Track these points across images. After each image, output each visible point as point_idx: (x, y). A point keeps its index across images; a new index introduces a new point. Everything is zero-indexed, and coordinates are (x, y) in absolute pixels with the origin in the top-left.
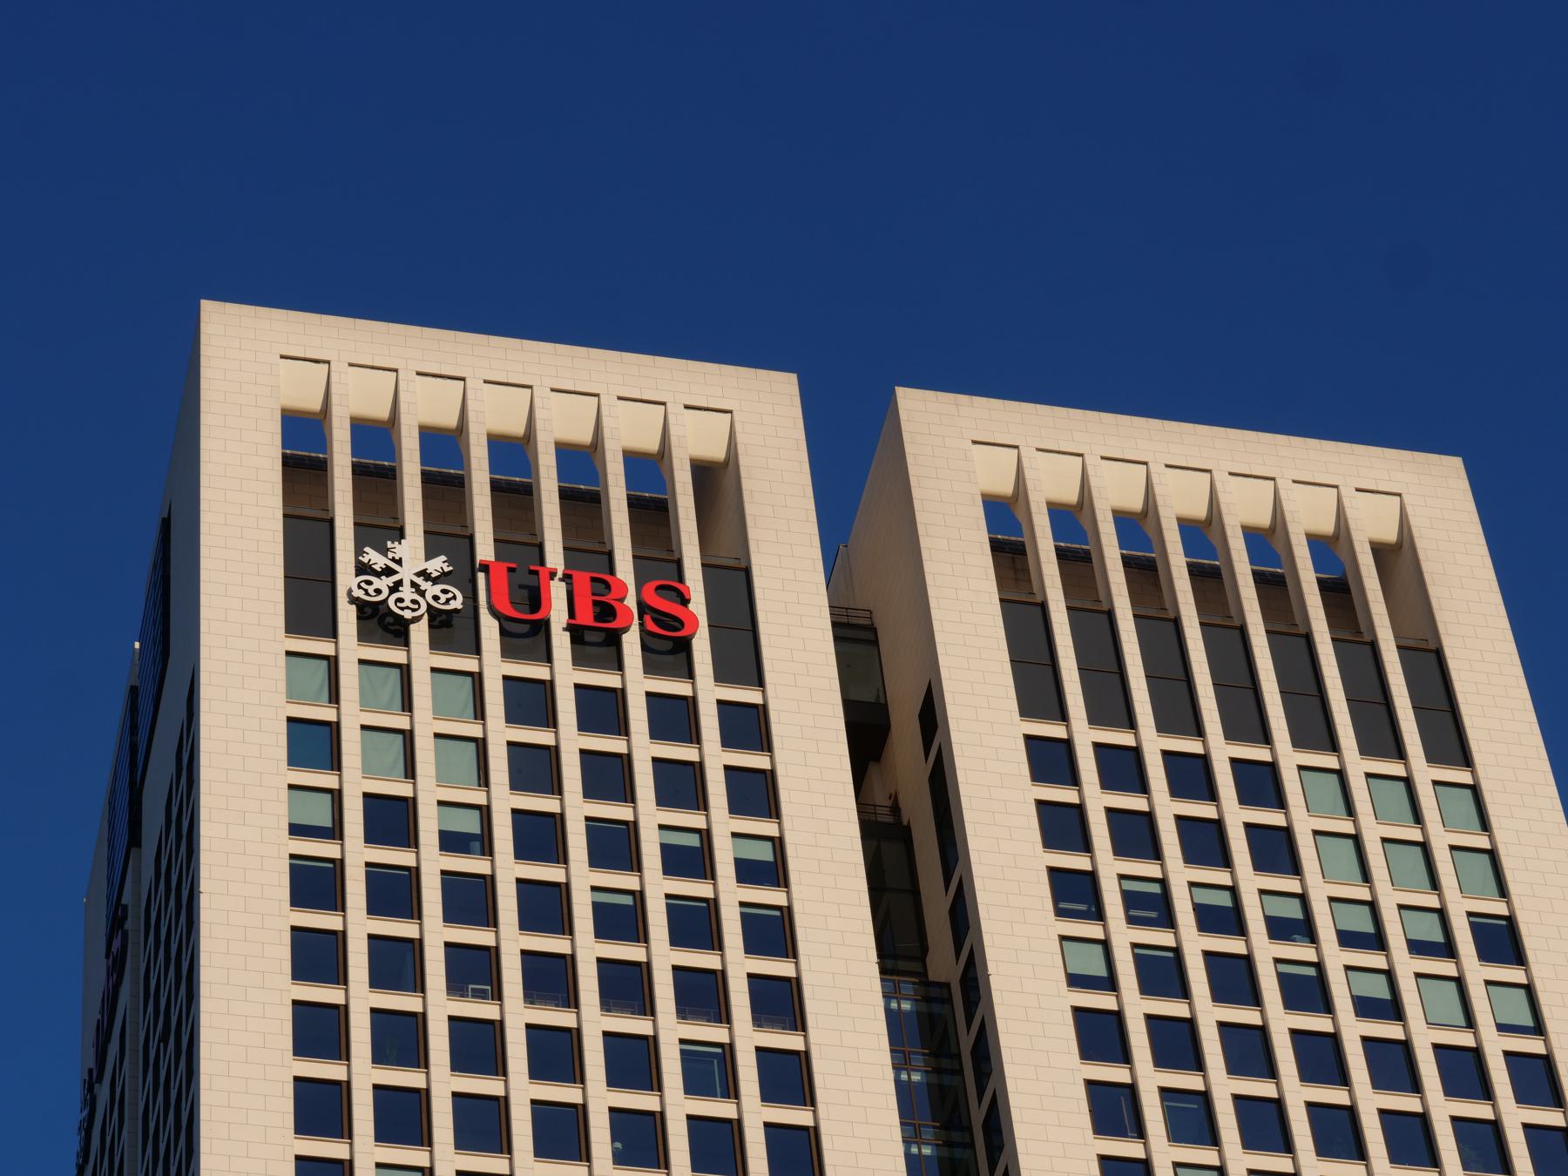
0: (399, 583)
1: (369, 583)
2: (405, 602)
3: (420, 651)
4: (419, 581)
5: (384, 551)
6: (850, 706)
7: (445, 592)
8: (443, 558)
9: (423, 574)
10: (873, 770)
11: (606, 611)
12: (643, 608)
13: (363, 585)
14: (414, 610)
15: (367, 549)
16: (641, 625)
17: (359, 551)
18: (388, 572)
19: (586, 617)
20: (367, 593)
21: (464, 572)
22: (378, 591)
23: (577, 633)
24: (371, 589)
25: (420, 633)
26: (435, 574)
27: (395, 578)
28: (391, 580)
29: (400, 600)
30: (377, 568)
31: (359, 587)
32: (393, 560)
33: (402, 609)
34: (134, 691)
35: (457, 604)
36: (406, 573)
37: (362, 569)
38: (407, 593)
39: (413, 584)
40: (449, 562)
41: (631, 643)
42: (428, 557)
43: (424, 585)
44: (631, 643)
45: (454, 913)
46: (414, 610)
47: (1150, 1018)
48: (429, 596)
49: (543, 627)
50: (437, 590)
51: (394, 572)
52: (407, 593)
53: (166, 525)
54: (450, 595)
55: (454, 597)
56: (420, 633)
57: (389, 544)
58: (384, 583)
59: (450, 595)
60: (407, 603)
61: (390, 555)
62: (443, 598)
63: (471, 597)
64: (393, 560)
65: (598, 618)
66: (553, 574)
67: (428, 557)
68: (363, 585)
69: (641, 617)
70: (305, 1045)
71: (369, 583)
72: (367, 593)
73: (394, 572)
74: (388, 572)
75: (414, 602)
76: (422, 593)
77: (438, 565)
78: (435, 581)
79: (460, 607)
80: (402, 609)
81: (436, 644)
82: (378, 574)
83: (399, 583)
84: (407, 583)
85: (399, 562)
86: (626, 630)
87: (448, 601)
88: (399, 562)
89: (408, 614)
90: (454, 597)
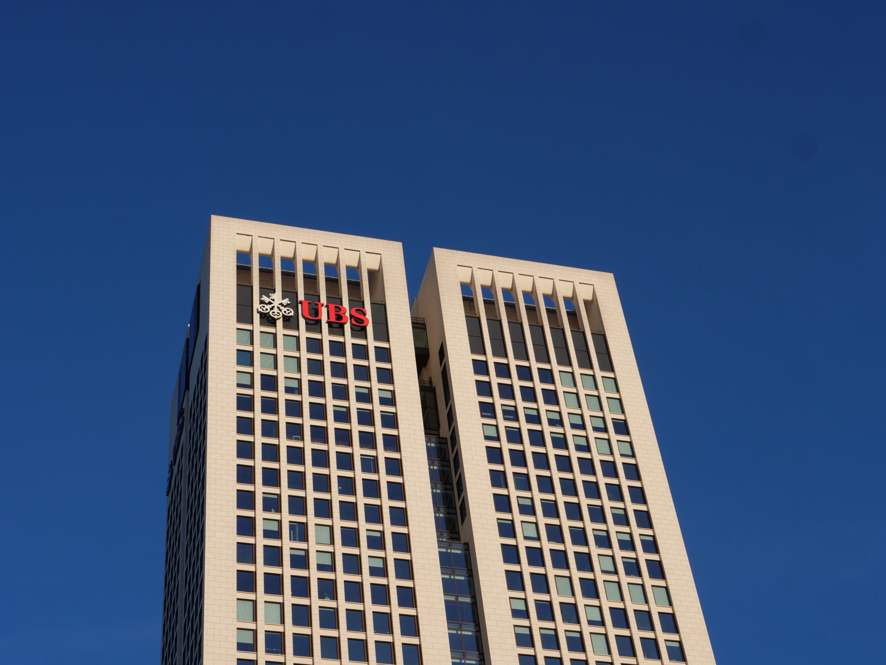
0: (273, 307)
1: (264, 307)
2: (275, 313)
4: (280, 306)
5: (269, 297)
6: (417, 349)
7: (288, 310)
8: (288, 299)
9: (281, 304)
10: (423, 369)
11: (339, 317)
12: (351, 316)
13: (262, 307)
14: (278, 316)
15: (263, 296)
16: (351, 322)
17: (261, 297)
18: (270, 303)
19: (333, 319)
20: (263, 310)
21: (294, 304)
22: (267, 309)
23: (330, 324)
24: (264, 309)
25: (280, 323)
26: (285, 304)
27: (272, 305)
28: (271, 306)
29: (274, 312)
30: (266, 302)
31: (261, 308)
32: (272, 299)
33: (274, 315)
34: (188, 340)
35: (292, 314)
36: (276, 304)
37: (262, 302)
38: (276, 310)
39: (278, 307)
40: (290, 300)
41: (347, 327)
42: (283, 298)
43: (282, 308)
44: (347, 327)
46: (278, 316)
47: (527, 548)
48: (283, 311)
49: (319, 322)
50: (285, 309)
51: (272, 303)
52: (276, 310)
53: (199, 287)
54: (290, 311)
55: (291, 312)
56: (280, 323)
57: (270, 294)
59: (290, 311)
60: (276, 313)
61: (271, 298)
62: (287, 312)
63: (297, 312)
64: (272, 299)
65: (336, 319)
66: (323, 305)
67: (283, 298)
68: (262, 307)
69: (350, 319)
70: (241, 559)
71: (264, 307)
72: (263, 310)
73: (272, 303)
74: (270, 303)
75: (278, 313)
76: (281, 310)
77: (286, 301)
79: (293, 315)
80: (274, 315)
81: (285, 327)
82: (267, 304)
83: (273, 307)
84: (276, 307)
85: (273, 300)
86: (346, 323)
87: (289, 313)
88: (273, 300)
89: (276, 317)
90: (291, 312)
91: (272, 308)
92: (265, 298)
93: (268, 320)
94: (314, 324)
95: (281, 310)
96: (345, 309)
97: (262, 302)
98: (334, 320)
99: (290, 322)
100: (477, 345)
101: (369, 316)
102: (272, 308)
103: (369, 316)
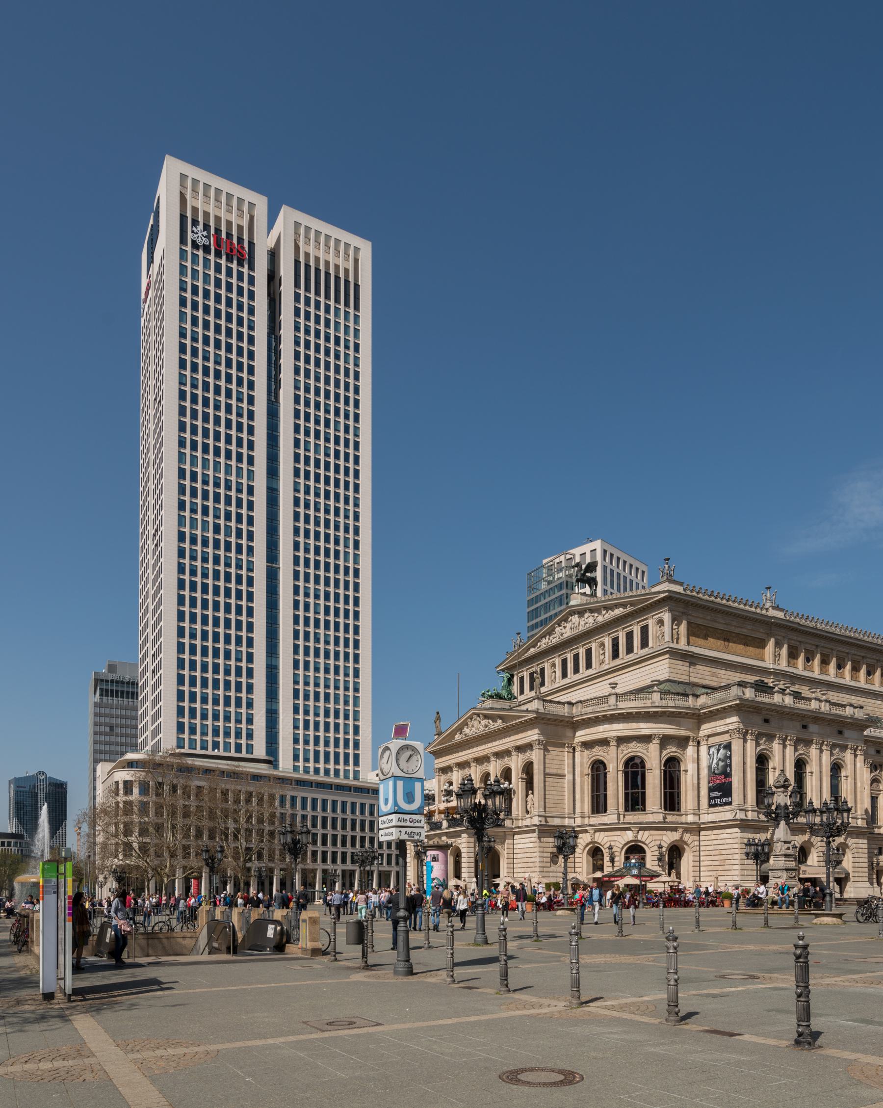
21: (208, 237)
35: (208, 244)
36: (200, 234)
37: (193, 232)
50: (204, 239)
58: (196, 236)
74: (197, 233)
77: (205, 233)
92: (194, 229)
93: (195, 245)
97: (193, 232)
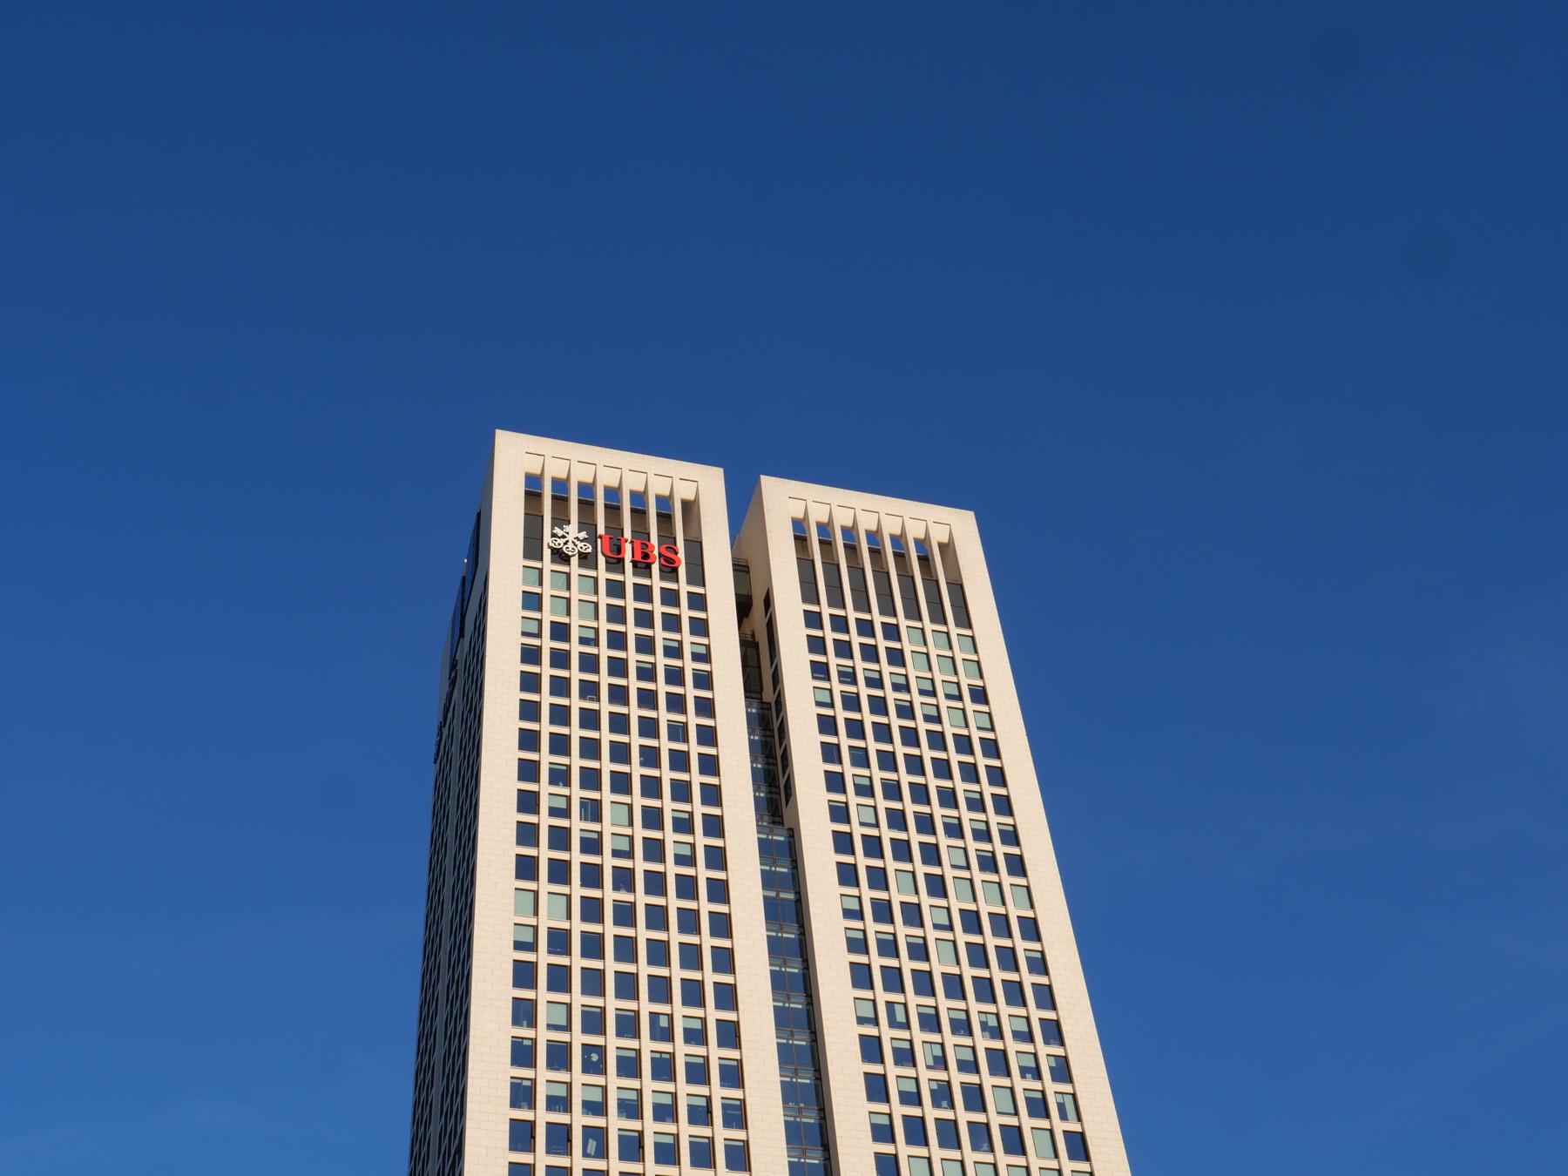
2: (569, 549)
3: (574, 567)
4: (575, 541)
5: (562, 529)
6: (738, 596)
9: (577, 538)
10: (745, 620)
11: (646, 556)
12: (660, 555)
17: (552, 529)
18: (564, 537)
19: (638, 558)
21: (593, 538)
22: (559, 544)
23: (635, 564)
24: (557, 543)
25: (575, 561)
28: (564, 540)
34: (464, 578)
35: (589, 550)
36: (570, 538)
37: (554, 535)
38: (570, 545)
40: (587, 534)
41: (655, 568)
42: (579, 532)
43: (577, 542)
44: (655, 568)
45: (584, 754)
48: (579, 547)
49: (621, 561)
50: (582, 544)
52: (570, 545)
53: (479, 515)
56: (575, 561)
58: (562, 541)
60: (570, 549)
62: (584, 548)
63: (595, 548)
65: (643, 558)
66: (626, 541)
67: (579, 532)
74: (564, 537)
76: (576, 546)
77: (583, 535)
78: (581, 541)
81: (581, 565)
82: (560, 538)
84: (570, 541)
85: (568, 533)
88: (568, 533)
89: (570, 554)
91: (566, 543)
92: (558, 531)
93: (560, 556)
94: (616, 563)
95: (576, 546)
96: (653, 546)
97: (554, 535)
98: (640, 560)
99: (587, 560)
100: (809, 593)
101: (681, 555)
102: (566, 543)
103: (681, 555)
